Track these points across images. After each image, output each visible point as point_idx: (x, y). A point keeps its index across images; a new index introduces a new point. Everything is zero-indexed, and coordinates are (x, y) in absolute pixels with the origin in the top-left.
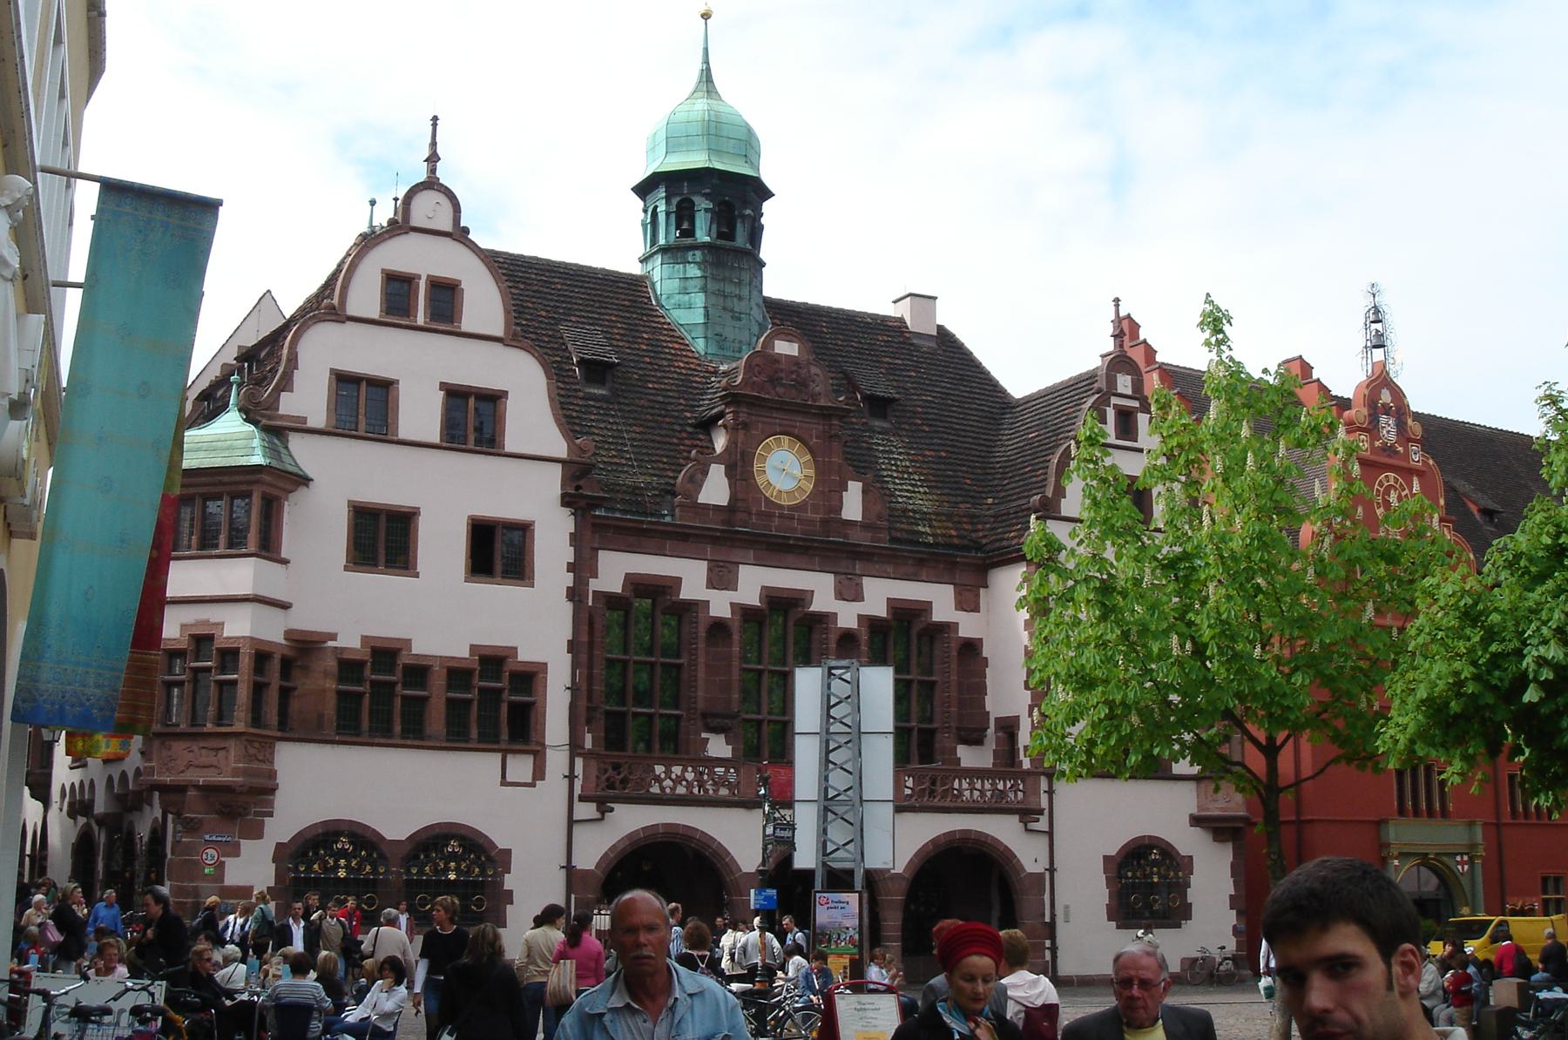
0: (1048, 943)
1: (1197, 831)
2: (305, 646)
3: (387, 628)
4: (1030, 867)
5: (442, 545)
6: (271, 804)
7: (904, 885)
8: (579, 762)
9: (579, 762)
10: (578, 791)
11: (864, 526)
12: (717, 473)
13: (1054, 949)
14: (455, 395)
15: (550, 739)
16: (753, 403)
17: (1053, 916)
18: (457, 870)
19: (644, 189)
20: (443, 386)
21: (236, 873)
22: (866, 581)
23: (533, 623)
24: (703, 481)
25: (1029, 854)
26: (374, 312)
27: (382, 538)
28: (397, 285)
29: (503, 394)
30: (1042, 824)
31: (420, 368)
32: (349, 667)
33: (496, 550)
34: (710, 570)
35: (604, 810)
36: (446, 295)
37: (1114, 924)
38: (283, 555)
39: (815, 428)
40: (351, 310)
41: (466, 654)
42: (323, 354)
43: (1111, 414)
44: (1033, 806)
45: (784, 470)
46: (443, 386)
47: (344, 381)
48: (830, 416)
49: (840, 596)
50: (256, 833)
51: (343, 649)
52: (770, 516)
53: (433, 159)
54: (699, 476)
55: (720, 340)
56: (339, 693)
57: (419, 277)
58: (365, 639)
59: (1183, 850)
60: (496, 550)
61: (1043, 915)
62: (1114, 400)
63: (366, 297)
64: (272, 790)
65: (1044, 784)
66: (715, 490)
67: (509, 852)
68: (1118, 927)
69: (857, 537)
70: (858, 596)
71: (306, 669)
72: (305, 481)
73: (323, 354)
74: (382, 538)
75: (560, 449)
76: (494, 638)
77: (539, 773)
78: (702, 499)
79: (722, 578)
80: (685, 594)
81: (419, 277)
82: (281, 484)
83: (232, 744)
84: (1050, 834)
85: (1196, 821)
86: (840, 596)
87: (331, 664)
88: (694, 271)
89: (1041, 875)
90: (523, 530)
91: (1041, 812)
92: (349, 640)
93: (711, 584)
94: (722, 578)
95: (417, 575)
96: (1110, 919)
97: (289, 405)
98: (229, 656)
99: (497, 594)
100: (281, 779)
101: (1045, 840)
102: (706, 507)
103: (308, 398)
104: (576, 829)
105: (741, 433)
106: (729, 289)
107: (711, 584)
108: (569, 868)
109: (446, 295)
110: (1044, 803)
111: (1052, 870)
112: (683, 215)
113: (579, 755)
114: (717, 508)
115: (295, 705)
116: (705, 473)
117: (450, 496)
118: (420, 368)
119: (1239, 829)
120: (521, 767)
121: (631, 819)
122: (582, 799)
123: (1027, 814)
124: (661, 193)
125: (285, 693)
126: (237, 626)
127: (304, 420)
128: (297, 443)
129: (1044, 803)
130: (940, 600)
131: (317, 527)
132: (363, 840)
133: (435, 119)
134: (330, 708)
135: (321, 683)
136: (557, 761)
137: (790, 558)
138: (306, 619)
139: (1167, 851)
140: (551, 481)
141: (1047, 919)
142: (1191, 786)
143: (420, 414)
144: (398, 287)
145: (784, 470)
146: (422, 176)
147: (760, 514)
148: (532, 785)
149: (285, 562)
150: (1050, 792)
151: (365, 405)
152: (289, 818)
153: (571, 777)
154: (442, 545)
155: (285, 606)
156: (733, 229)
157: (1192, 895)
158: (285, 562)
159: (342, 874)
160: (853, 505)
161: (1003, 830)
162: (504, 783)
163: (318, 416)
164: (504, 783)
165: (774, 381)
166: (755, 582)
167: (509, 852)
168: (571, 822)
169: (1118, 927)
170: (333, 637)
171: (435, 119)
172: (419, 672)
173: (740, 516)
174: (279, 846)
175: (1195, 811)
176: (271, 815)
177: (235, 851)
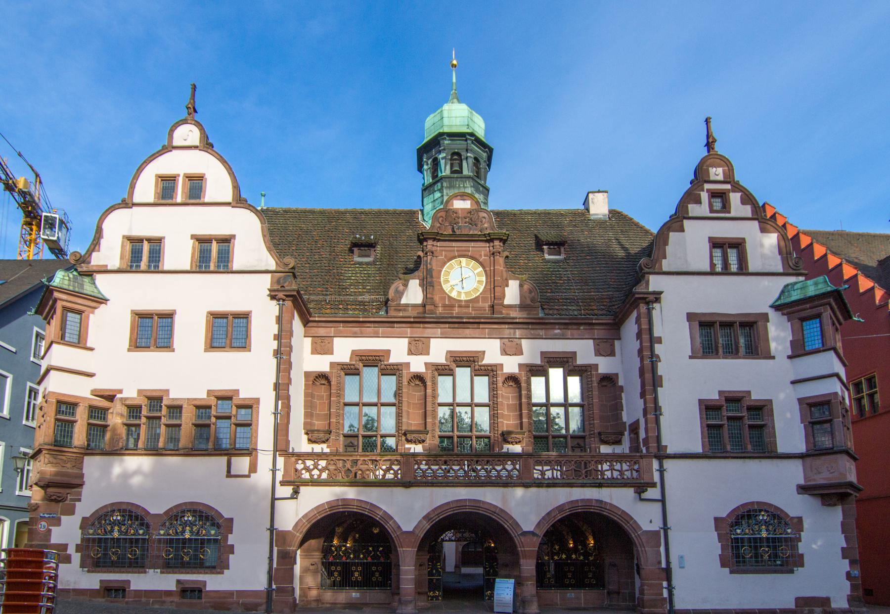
0: (665, 584)
3: (153, 384)
4: (646, 526)
5: (190, 331)
6: (80, 494)
7: (537, 541)
9: (281, 461)
14: (203, 241)
17: (668, 562)
18: (191, 532)
20: (193, 237)
21: (57, 536)
25: (644, 517)
27: (152, 330)
28: (166, 184)
29: (234, 236)
30: (653, 493)
33: (227, 331)
35: (296, 492)
36: (196, 184)
38: (89, 345)
40: (136, 200)
41: (205, 396)
43: (704, 196)
44: (646, 481)
46: (193, 237)
51: (126, 399)
57: (179, 175)
58: (140, 392)
59: (792, 513)
60: (227, 331)
61: (660, 562)
62: (707, 186)
65: (655, 464)
67: (231, 520)
68: (731, 572)
72: (103, 301)
75: (272, 264)
76: (223, 385)
77: (253, 468)
81: (179, 175)
84: (663, 501)
85: (803, 489)
89: (657, 533)
90: (245, 316)
91: (654, 485)
92: (130, 393)
95: (173, 350)
96: (723, 565)
97: (97, 259)
101: (659, 505)
103: (110, 252)
108: (272, 529)
110: (656, 477)
111: (666, 528)
117: (192, 299)
118: (178, 230)
119: (847, 495)
122: (283, 483)
123: (640, 487)
127: (106, 266)
128: (99, 278)
129: (656, 477)
131: (109, 327)
132: (132, 514)
136: (265, 460)
138: (103, 383)
141: (664, 565)
143: (178, 253)
144: (167, 184)
149: (92, 349)
150: (662, 471)
152: (89, 503)
153: (274, 471)
154: (190, 331)
155: (91, 375)
157: (802, 548)
158: (92, 349)
159: (116, 534)
161: (621, 499)
162: (229, 474)
163: (115, 263)
167: (231, 520)
168: (274, 499)
169: (731, 572)
170: (121, 391)
171: (194, 88)
172: (176, 409)
174: (84, 518)
175: (802, 482)
176: (79, 500)
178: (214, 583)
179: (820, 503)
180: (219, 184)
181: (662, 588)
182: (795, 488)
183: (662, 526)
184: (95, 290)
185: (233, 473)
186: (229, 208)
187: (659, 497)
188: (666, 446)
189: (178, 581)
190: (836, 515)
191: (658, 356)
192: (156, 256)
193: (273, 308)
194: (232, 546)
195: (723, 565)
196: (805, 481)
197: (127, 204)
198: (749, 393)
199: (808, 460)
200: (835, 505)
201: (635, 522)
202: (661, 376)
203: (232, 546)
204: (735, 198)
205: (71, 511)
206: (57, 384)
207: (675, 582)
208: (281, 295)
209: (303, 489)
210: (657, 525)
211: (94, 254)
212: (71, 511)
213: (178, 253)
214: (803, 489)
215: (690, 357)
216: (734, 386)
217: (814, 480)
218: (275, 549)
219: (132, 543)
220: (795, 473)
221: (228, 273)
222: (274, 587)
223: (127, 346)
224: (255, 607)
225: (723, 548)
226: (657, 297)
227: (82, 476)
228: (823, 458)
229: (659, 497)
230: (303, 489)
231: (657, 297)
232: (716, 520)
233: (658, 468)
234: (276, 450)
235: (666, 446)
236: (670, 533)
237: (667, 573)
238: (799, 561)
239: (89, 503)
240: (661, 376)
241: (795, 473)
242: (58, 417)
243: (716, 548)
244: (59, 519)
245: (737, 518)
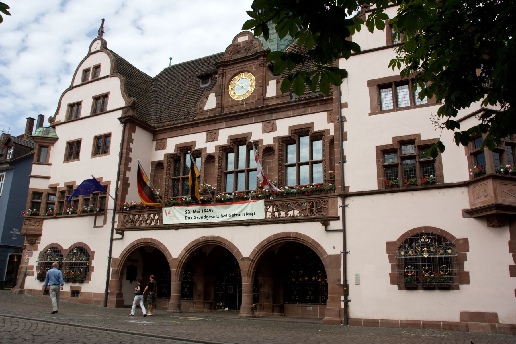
0: (343, 298)
1: (471, 222)
8: (117, 216)
10: (115, 227)
11: (277, 97)
13: (347, 302)
14: (96, 99)
15: (109, 208)
22: (278, 122)
24: (206, 101)
25: (328, 243)
29: (109, 93)
30: (334, 225)
32: (63, 193)
34: (207, 135)
35: (123, 235)
37: (396, 286)
38: (50, 162)
39: (254, 65)
47: (71, 106)
48: (257, 58)
49: (265, 131)
50: (36, 249)
52: (233, 106)
53: (101, 32)
54: (205, 100)
56: (59, 202)
61: (340, 280)
64: (40, 235)
65: (339, 201)
66: (211, 103)
67: (94, 252)
69: (271, 103)
70: (273, 129)
77: (105, 222)
78: (206, 108)
79: (212, 137)
80: (197, 147)
82: (46, 141)
85: (469, 213)
86: (265, 131)
89: (338, 257)
91: (338, 218)
93: (207, 141)
94: (212, 137)
100: (44, 232)
101: (341, 235)
102: (207, 111)
104: (114, 242)
105: (220, 77)
107: (207, 141)
108: (110, 257)
111: (345, 253)
113: (117, 213)
116: (207, 98)
120: (100, 220)
121: (132, 237)
133: (103, 20)
137: (242, 121)
139: (438, 237)
141: (342, 283)
142: (465, 190)
145: (242, 86)
147: (229, 107)
148: (102, 226)
149: (50, 165)
150: (344, 207)
151: (74, 111)
152: (43, 244)
153: (113, 222)
155: (49, 178)
157: (467, 266)
158: (50, 165)
160: (272, 89)
161: (311, 231)
162: (95, 226)
164: (95, 226)
166: (224, 136)
167: (94, 252)
168: (112, 240)
170: (58, 185)
173: (217, 110)
175: (468, 207)
178: (86, 288)
179: (486, 226)
181: (341, 301)
182: (461, 212)
183: (342, 251)
184: (55, 134)
185: (97, 225)
186: (108, 79)
187: (341, 228)
188: (349, 187)
189: (71, 287)
190: (504, 237)
191: (344, 117)
194: (93, 267)
195: (393, 282)
196: (470, 206)
198: (419, 135)
199: (471, 187)
200: (506, 226)
201: (322, 248)
202: (346, 132)
203: (93, 267)
206: (35, 184)
207: (350, 297)
208: (123, 120)
209: (126, 233)
210: (338, 250)
211: (57, 116)
214: (469, 213)
215: (370, 114)
216: (406, 131)
217: (476, 204)
218: (111, 269)
219: (79, 265)
220: (462, 199)
221: (104, 113)
222: (109, 291)
223: (63, 161)
224: (98, 302)
225: (393, 268)
226: (344, 74)
227: (41, 230)
228: (480, 183)
229: (341, 228)
230: (126, 233)
231: (344, 74)
232: (388, 244)
233: (341, 204)
234: (115, 210)
235: (349, 187)
236: (348, 256)
237: (345, 289)
238: (465, 278)
239: (43, 244)
240: (346, 132)
241: (462, 199)
243: (387, 268)
244: (32, 253)
245: (406, 241)
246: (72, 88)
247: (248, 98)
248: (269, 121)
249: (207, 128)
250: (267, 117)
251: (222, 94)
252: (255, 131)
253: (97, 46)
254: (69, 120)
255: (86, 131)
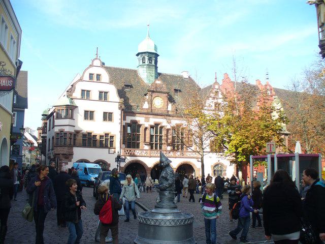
2: (78, 132)
5: (98, 116)
12: (146, 103)
14: (101, 92)
16: (153, 92)
19: (138, 55)
23: (114, 128)
26: (88, 79)
27: (89, 115)
31: (95, 89)
32: (84, 135)
33: (108, 116)
36: (98, 76)
42: (80, 87)
45: (159, 102)
55: (149, 80)
60: (108, 116)
63: (86, 77)
66: (146, 106)
71: (78, 136)
72: (77, 107)
73: (80, 87)
74: (89, 115)
76: (107, 132)
79: (147, 120)
83: (66, 147)
87: (82, 135)
88: (145, 69)
94: (147, 120)
98: (65, 134)
99: (108, 123)
103: (77, 94)
106: (151, 72)
109: (98, 76)
112: (143, 59)
114: (146, 109)
115: (76, 141)
117: (99, 108)
124: (140, 56)
125: (75, 139)
126: (67, 129)
130: (184, 123)
134: (81, 142)
135: (80, 138)
140: (117, 105)
143: (95, 95)
144: (91, 75)
146: (95, 57)
151: (86, 94)
154: (98, 116)
156: (152, 61)
163: (79, 96)
165: (156, 88)
166: (153, 121)
177: (67, 164)
180: (105, 77)
192: (88, 95)
193: (119, 112)
197: (81, 80)
204: (220, 93)
205: (70, 161)
212: (70, 161)
213: (95, 95)
242: (109, 146)
246: (81, 80)
247: (161, 108)
248: (169, 119)
249: (145, 116)
250: (168, 118)
251: (151, 103)
252: (163, 122)
253: (97, 63)
254: (82, 98)
255: (99, 108)
